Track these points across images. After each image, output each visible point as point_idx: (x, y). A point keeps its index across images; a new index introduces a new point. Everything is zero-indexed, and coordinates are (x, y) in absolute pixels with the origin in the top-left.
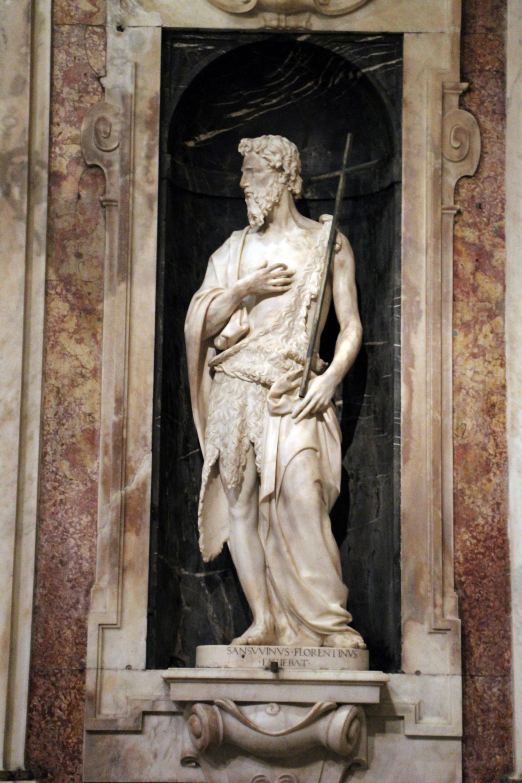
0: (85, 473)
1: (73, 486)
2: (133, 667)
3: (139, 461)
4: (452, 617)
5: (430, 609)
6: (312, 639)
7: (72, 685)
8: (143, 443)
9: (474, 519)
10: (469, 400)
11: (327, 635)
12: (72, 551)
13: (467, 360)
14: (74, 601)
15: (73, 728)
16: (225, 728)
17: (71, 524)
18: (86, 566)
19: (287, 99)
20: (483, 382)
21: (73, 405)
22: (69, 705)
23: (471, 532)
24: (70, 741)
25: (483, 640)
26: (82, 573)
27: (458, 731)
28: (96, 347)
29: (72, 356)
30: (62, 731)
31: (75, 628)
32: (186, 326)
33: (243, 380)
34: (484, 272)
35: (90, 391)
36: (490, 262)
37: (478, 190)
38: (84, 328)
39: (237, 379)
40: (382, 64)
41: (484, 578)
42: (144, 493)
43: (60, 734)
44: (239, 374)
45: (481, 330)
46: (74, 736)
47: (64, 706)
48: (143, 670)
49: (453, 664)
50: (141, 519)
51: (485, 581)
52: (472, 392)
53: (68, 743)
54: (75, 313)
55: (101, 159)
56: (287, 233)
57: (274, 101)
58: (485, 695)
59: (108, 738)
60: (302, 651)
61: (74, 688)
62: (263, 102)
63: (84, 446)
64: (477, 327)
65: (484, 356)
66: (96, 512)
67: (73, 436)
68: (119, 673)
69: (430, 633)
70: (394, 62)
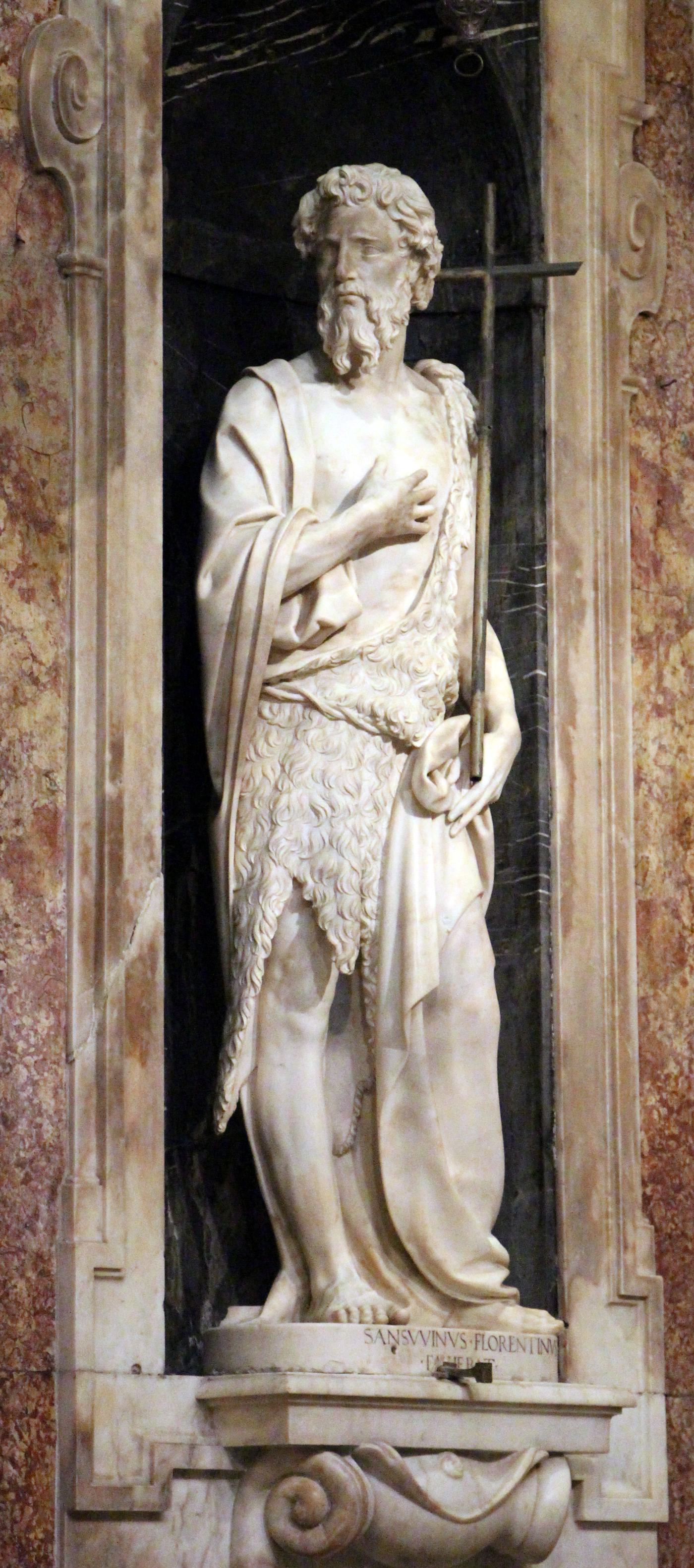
0: (42, 911)
1: (21, 941)
2: (144, 1370)
3: (141, 892)
4: (646, 1271)
5: (610, 1255)
6: (434, 1313)
7: (32, 1406)
8: (148, 854)
9: (663, 1065)
10: (653, 806)
11: (468, 1305)
12: (24, 1095)
13: (647, 719)
14: (30, 1212)
15: (36, 1506)
16: (376, 1507)
17: (18, 1029)
18: (49, 1132)
19: (260, 54)
20: (672, 769)
21: (18, 749)
22: (28, 1453)
23: (660, 1090)
24: (32, 1536)
25: (680, 1320)
26: (43, 1148)
27: (661, 1514)
28: (57, 615)
29: (13, 629)
30: (17, 1513)
31: (31, 1275)
32: (204, 586)
33: (358, 726)
34: (669, 528)
35: (48, 718)
36: (678, 509)
37: (657, 346)
38: (35, 565)
39: (343, 725)
40: (507, 29)
41: (679, 1188)
42: (153, 969)
43: (14, 1521)
44: (354, 714)
45: (667, 656)
46: (39, 1523)
47: (19, 1455)
48: (162, 1376)
49: (649, 1370)
50: (148, 1027)
51: (681, 1196)
52: (656, 789)
53: (28, 1539)
54: (18, 527)
55: (66, 158)
56: (399, 397)
57: (238, 53)
58: (683, 1436)
59: (106, 1527)
60: (486, 1339)
61: (35, 1414)
62: (219, 52)
63: (35, 847)
64: (662, 649)
65: (672, 712)
66: (67, 1007)
67: (18, 822)
68: (121, 1380)
69: (612, 1304)
70: (521, 27)
